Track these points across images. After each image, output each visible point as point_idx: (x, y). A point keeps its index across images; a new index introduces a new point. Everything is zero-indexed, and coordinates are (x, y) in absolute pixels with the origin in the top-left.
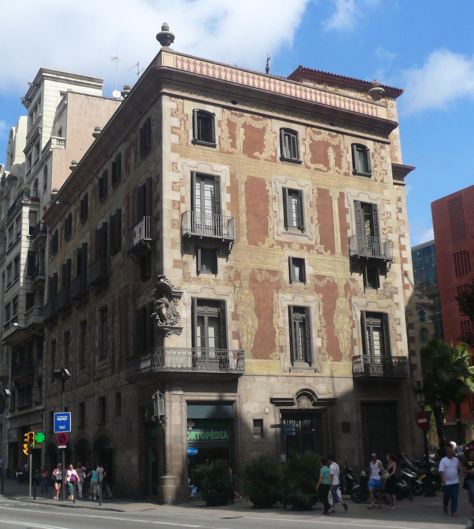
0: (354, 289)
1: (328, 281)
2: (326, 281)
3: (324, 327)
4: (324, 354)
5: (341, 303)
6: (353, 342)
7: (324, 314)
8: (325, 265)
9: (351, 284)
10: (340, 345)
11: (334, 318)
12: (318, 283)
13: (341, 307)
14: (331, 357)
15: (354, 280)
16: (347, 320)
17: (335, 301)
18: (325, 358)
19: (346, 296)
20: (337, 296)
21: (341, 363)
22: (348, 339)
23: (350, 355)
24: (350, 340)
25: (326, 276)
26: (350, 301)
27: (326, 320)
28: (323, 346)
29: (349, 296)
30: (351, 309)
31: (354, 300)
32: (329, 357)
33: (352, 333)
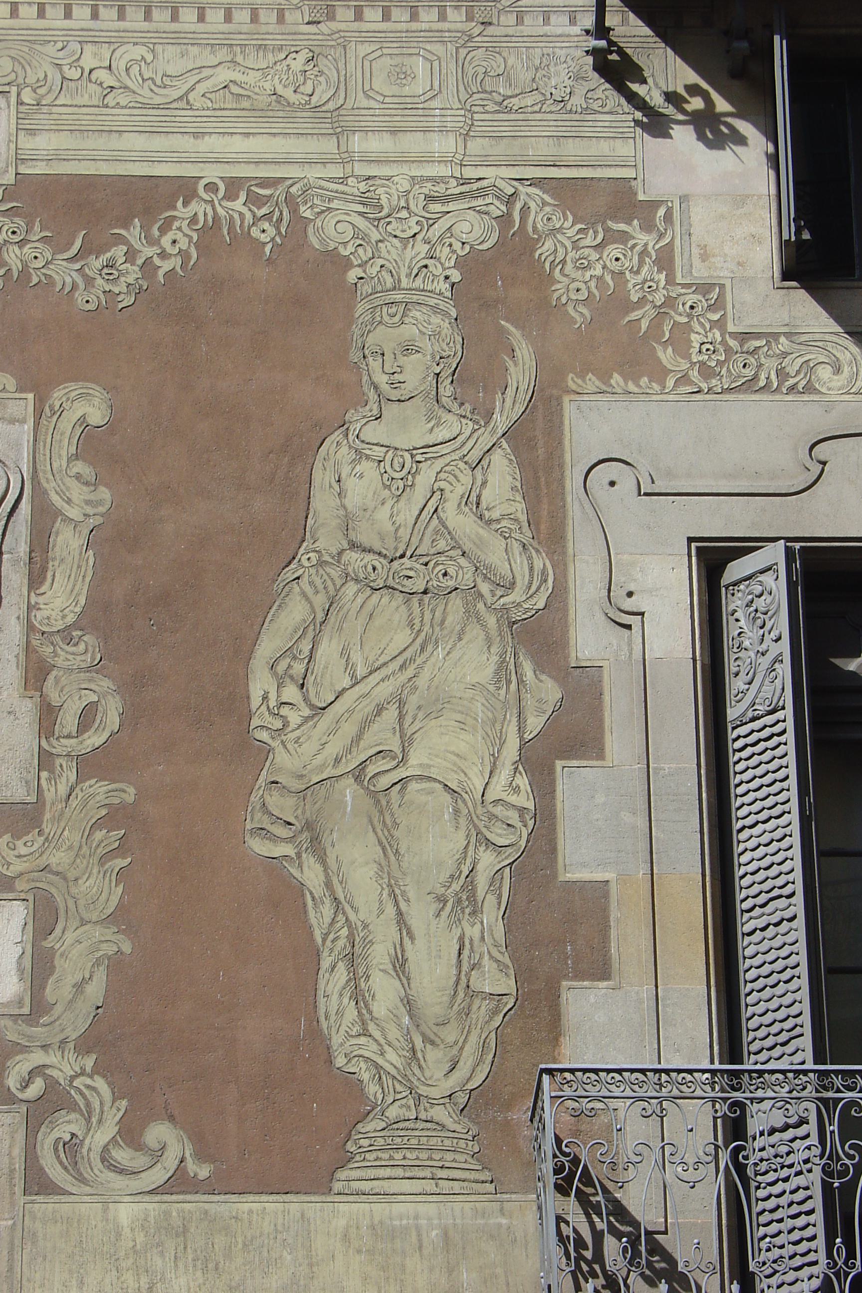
0: (613, 303)
1: (209, 233)
2: (179, 239)
3: (89, 766)
4: (54, 1101)
5: (393, 469)
6: (554, 935)
7: (97, 616)
8: (171, 61)
9: (560, 238)
10: (333, 983)
11: (268, 647)
12: (64, 273)
13: (389, 518)
14: (158, 1132)
15: (616, 204)
16: (469, 662)
17: (299, 450)
18: (70, 1148)
19: (470, 379)
20: (344, 391)
21: (331, 1218)
22: (467, 902)
23: (476, 1103)
24: (492, 914)
25: (186, 189)
26: (536, 443)
27: (133, 686)
28: (37, 1007)
29: (521, 373)
30: (547, 530)
31: (593, 423)
32: (130, 1133)
33: (544, 819)
